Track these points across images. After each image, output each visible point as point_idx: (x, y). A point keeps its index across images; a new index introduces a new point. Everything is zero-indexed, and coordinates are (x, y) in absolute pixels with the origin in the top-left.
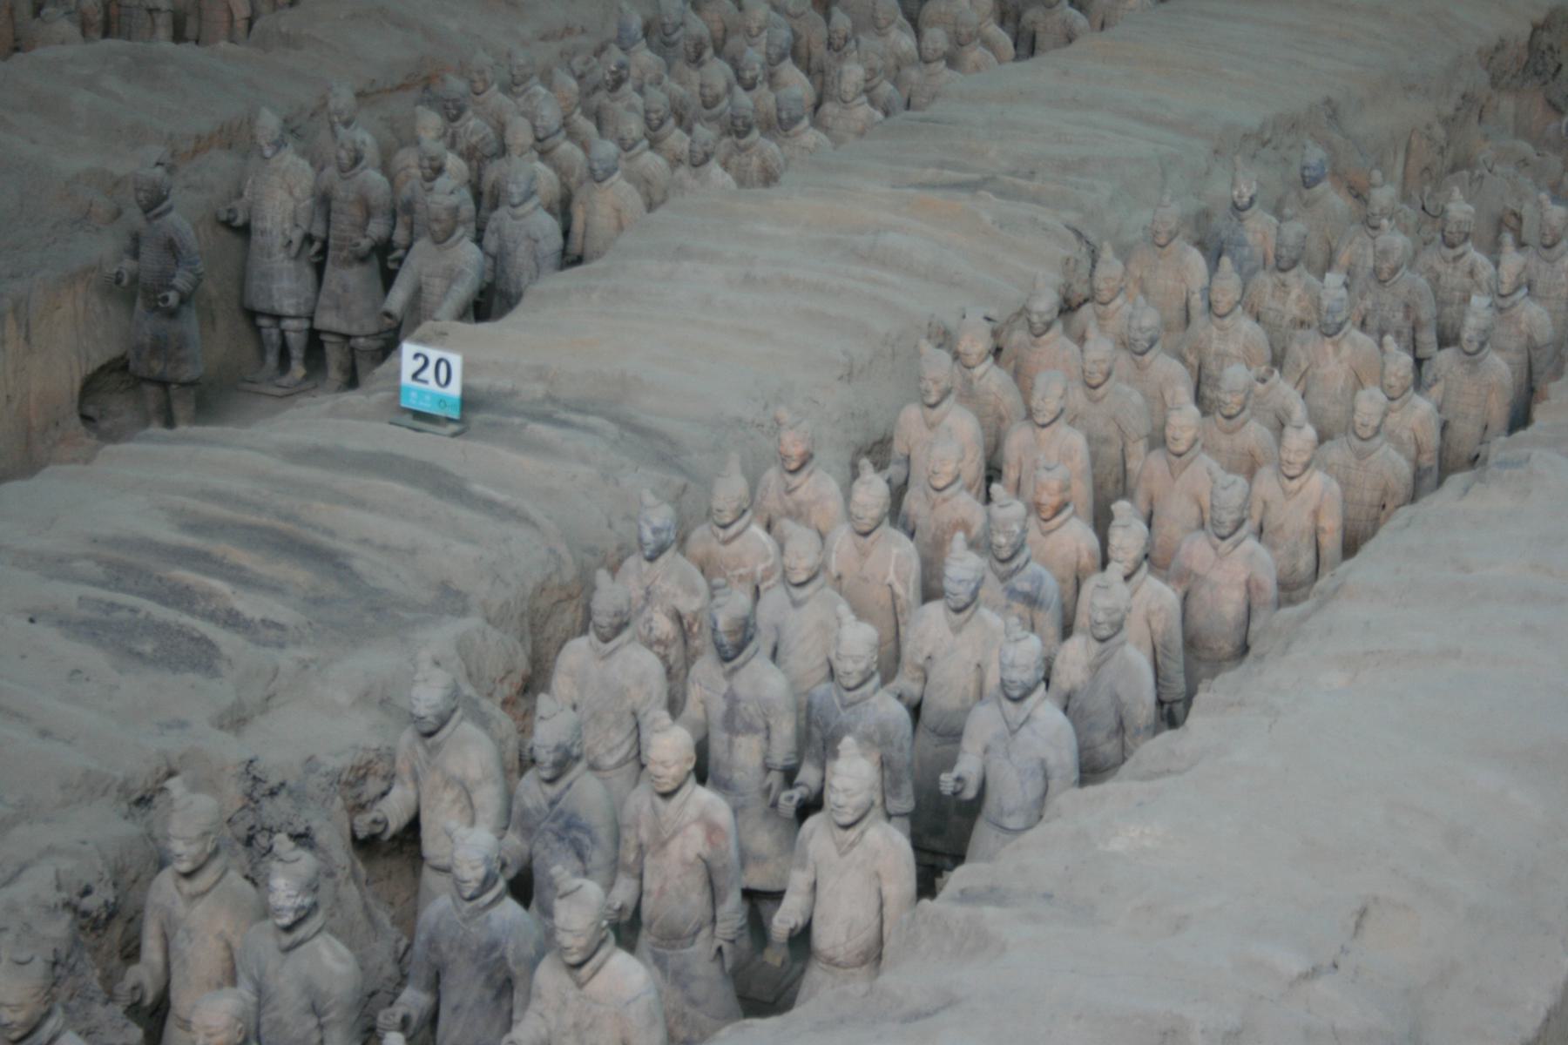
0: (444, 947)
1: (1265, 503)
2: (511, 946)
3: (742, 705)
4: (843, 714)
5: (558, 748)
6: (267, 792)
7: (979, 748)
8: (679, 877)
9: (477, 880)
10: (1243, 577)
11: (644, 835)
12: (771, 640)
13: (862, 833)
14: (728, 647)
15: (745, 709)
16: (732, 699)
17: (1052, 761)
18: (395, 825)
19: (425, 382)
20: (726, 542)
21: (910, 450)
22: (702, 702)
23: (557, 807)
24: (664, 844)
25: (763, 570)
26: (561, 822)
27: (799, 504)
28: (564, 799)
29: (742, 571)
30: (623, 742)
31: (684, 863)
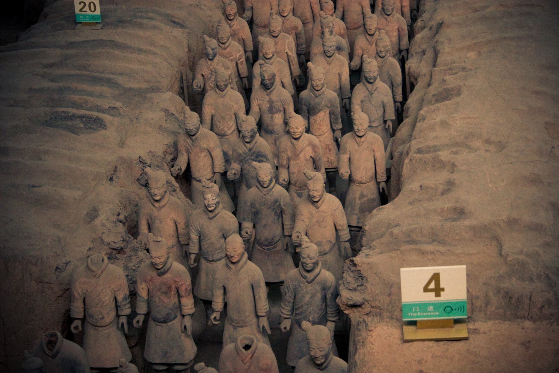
0: (257, 206)
2: (282, 200)
3: (275, 104)
4: (316, 99)
5: (251, 131)
7: (359, 102)
8: (305, 165)
9: (268, 180)
10: (397, 27)
11: (289, 154)
13: (366, 137)
14: (269, 85)
16: (271, 102)
17: (386, 102)
18: (184, 168)
19: (86, 11)
20: (225, 49)
21: (252, 5)
22: (258, 105)
24: (298, 155)
27: (234, 31)
28: (255, 147)
29: (232, 58)
30: (233, 125)
31: (306, 160)
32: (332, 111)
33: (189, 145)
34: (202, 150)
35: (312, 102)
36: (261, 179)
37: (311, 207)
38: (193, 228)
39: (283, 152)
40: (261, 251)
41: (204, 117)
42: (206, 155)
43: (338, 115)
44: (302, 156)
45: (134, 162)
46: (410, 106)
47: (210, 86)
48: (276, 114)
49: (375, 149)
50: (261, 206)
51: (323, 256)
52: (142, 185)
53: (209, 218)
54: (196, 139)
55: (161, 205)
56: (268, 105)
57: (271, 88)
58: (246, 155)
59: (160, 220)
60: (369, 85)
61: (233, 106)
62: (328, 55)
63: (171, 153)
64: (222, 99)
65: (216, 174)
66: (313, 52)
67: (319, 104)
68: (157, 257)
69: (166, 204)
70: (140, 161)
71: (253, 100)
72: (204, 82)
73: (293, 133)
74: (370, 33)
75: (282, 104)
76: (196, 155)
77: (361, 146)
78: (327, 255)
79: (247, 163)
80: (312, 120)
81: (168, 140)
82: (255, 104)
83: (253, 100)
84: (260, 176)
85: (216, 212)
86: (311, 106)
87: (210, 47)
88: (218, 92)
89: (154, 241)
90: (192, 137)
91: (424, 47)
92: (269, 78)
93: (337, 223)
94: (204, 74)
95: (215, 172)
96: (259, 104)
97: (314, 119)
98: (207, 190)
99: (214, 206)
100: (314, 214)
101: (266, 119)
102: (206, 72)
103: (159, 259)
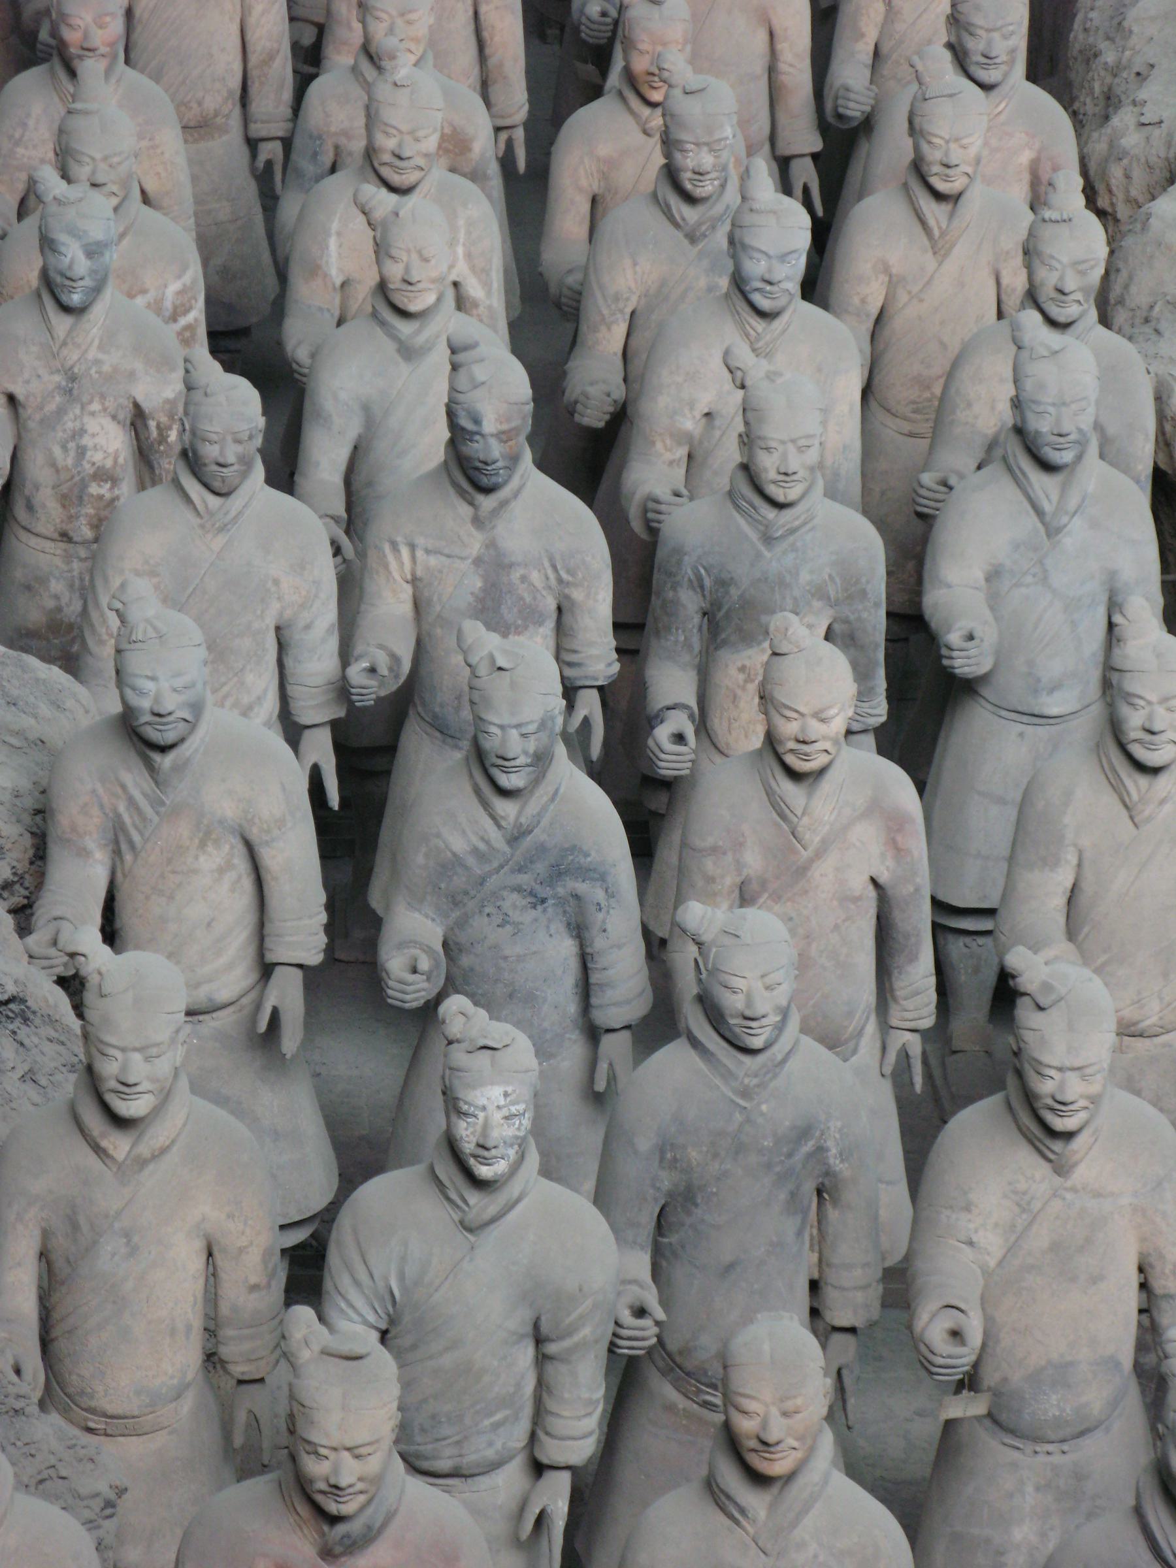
0: (694, 1154)
2: (834, 1125)
3: (516, 575)
5: (543, 725)
7: (978, 574)
8: (836, 927)
10: (1025, 157)
12: (353, 430)
14: (500, 464)
15: (524, 579)
22: (414, 581)
23: (528, 841)
24: (802, 871)
25: (180, 293)
26: (541, 867)
28: (544, 822)
31: (848, 899)
32: (847, 621)
33: (132, 802)
34: (208, 833)
36: (733, 1002)
37: (1025, 1156)
38: (357, 1283)
39: (714, 850)
40: (687, 1414)
42: (228, 866)
43: (877, 646)
44: (824, 874)
47: (53, 464)
48: (519, 634)
50: (716, 1156)
51: (1065, 1447)
53: (461, 1222)
54: (179, 768)
55: (144, 1150)
56: (479, 584)
57: (506, 482)
58: (487, 868)
59: (127, 1235)
61: (276, 582)
62: (764, 303)
64: (219, 541)
65: (279, 970)
67: (782, 583)
68: (348, 1449)
69: (173, 1142)
71: (387, 548)
72: (19, 437)
73: (792, 745)
74: (941, 186)
75: (552, 576)
76: (169, 861)
77: (1149, 819)
78: (1087, 1442)
79: (487, 910)
80: (733, 671)
83: (387, 548)
85: (514, 1189)
86: (734, 592)
88: (194, 496)
89: (326, 1352)
90: (156, 757)
92: (505, 427)
93: (1161, 1256)
94: (19, 391)
95: (271, 958)
96: (419, 573)
97: (742, 669)
99: (512, 1153)
100: (1036, 1205)
103: (357, 1457)
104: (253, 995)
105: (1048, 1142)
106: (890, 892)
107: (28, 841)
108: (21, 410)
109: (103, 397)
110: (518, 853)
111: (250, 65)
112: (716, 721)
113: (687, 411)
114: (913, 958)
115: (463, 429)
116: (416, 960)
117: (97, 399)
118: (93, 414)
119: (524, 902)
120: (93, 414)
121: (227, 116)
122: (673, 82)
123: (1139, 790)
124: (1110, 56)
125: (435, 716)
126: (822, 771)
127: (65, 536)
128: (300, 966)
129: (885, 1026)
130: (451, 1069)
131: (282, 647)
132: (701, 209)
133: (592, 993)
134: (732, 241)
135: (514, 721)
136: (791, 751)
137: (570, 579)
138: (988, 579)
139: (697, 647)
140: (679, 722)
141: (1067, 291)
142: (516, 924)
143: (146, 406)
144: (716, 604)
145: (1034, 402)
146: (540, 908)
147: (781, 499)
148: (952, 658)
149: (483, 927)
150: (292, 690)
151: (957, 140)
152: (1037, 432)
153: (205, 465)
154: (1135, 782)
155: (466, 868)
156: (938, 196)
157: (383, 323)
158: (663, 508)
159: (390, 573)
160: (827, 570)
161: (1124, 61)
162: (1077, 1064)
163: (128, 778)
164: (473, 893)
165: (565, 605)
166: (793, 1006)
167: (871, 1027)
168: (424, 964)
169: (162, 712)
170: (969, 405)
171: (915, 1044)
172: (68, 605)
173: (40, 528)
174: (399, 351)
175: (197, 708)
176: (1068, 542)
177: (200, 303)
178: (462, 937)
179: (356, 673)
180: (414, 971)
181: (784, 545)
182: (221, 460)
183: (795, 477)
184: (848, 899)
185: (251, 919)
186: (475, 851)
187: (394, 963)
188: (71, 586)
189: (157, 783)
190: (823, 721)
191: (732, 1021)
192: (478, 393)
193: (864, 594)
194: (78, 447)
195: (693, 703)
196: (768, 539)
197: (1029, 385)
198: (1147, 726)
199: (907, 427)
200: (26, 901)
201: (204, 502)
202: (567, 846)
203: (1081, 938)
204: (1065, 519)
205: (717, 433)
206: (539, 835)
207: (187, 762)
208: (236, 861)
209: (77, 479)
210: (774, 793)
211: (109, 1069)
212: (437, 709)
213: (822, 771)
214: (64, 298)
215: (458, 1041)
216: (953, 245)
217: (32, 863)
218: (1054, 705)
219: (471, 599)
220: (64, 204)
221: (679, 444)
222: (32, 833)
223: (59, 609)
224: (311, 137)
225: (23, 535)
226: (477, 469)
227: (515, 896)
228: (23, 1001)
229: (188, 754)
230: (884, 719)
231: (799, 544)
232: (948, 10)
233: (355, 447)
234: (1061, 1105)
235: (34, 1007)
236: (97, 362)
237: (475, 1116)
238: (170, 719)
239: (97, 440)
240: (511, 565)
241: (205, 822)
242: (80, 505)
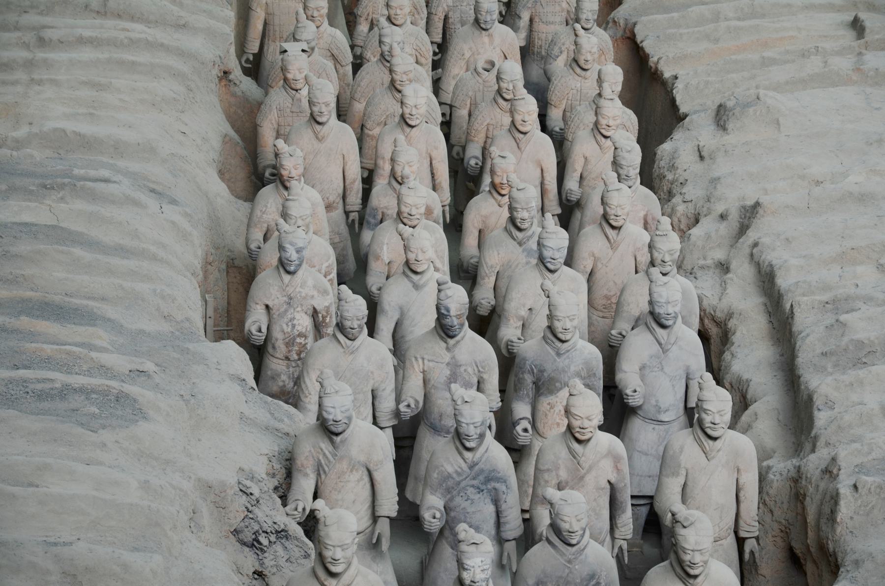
1: (586, 158)
2: (604, 574)
3: (462, 369)
6: (256, 502)
7: (637, 368)
8: (595, 500)
10: (642, 214)
14: (457, 327)
15: (465, 370)
16: (454, 366)
22: (424, 372)
23: (477, 468)
24: (582, 478)
25: (327, 267)
26: (481, 478)
28: (484, 459)
33: (324, 454)
34: (354, 467)
35: (549, 367)
36: (565, 526)
39: (548, 470)
41: (306, 397)
42: (361, 479)
44: (590, 479)
45: (230, 492)
46: (745, 376)
47: (283, 331)
49: (741, 467)
52: (244, 544)
54: (342, 442)
56: (449, 372)
57: (459, 334)
58: (461, 478)
60: (659, 331)
61: (372, 373)
62: (551, 267)
63: (274, 474)
64: (351, 357)
66: (487, 260)
67: (564, 371)
70: (241, 490)
71: (413, 359)
72: (270, 320)
73: (578, 429)
74: (614, 223)
76: (339, 478)
77: (713, 458)
79: (461, 494)
80: (545, 404)
81: (269, 446)
82: (417, 370)
84: (566, 518)
86: (545, 374)
87: (292, 244)
90: (335, 438)
91: (719, 255)
92: (459, 313)
94: (271, 305)
95: (378, 514)
96: (425, 369)
97: (549, 404)
98: (473, 547)
101: (440, 402)
102: (275, 298)
104: (370, 529)
105: (687, 579)
106: (615, 486)
107: (284, 471)
108: (271, 311)
109: (302, 305)
110: (473, 472)
111: (346, 184)
112: (539, 424)
113: (522, 308)
114: (624, 512)
115: (443, 314)
116: (435, 514)
117: (300, 306)
118: (298, 312)
119: (475, 491)
120: (298, 312)
121: (337, 203)
122: (513, 186)
123: (709, 447)
124: (670, 176)
125: (431, 423)
126: (589, 440)
127: (287, 358)
128: (388, 517)
129: (613, 538)
130: (460, 552)
131: (374, 397)
132: (523, 233)
133: (501, 526)
134: (539, 244)
135: (472, 422)
136: (578, 432)
137: (483, 371)
138: (640, 370)
139: (531, 396)
140: (525, 424)
141: (666, 261)
142: (472, 500)
143: (318, 308)
144: (539, 379)
145: (658, 302)
146: (481, 493)
147: (564, 339)
148: (628, 399)
149: (458, 501)
150: (377, 414)
151: (620, 206)
152: (659, 313)
153: (346, 329)
154: (708, 443)
155: (453, 478)
156: (613, 227)
157: (407, 276)
158: (514, 344)
159: (414, 369)
160: (580, 367)
161: (675, 178)
162: (699, 549)
163: (323, 446)
164: (455, 488)
165: (481, 380)
166: (587, 528)
167: (608, 538)
168: (438, 515)
169: (338, 420)
170: (629, 305)
171: (625, 546)
172: (288, 384)
173: (278, 355)
174: (413, 286)
175: (350, 418)
176: (670, 354)
177: (335, 271)
178: (452, 505)
179: (402, 407)
180: (434, 518)
181: (565, 356)
182: (352, 327)
183: (568, 331)
184: (599, 489)
185: (369, 499)
186: (456, 472)
187: (427, 515)
188: (289, 377)
189: (334, 448)
190: (590, 420)
191: (564, 534)
192: (448, 301)
193: (595, 374)
194: (292, 324)
195: (530, 416)
196: (558, 354)
197: (655, 295)
198: (713, 421)
199: (601, 314)
200: (283, 494)
201: (345, 343)
202: (491, 469)
203: (687, 504)
204: (670, 346)
205: (534, 316)
206: (481, 466)
207: (346, 439)
208: (364, 477)
209: (292, 336)
210: (571, 448)
211: (328, 554)
212: (432, 421)
213: (589, 440)
214: (288, 268)
215: (463, 541)
216: (619, 246)
217: (285, 480)
218: (664, 417)
219: (445, 378)
220: (288, 233)
221: (519, 320)
222: (285, 468)
223: (284, 386)
224: (373, 209)
225: (271, 358)
226: (448, 329)
227: (472, 489)
228: (286, 531)
229: (346, 436)
230: (602, 422)
231: (570, 356)
232: (612, 160)
233: (397, 323)
234: (693, 565)
235: (291, 534)
236: (300, 292)
237: (470, 570)
238: (340, 423)
239: (300, 322)
240: (460, 366)
241: (353, 462)
242: (293, 346)
